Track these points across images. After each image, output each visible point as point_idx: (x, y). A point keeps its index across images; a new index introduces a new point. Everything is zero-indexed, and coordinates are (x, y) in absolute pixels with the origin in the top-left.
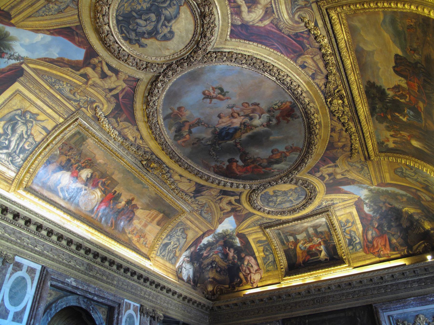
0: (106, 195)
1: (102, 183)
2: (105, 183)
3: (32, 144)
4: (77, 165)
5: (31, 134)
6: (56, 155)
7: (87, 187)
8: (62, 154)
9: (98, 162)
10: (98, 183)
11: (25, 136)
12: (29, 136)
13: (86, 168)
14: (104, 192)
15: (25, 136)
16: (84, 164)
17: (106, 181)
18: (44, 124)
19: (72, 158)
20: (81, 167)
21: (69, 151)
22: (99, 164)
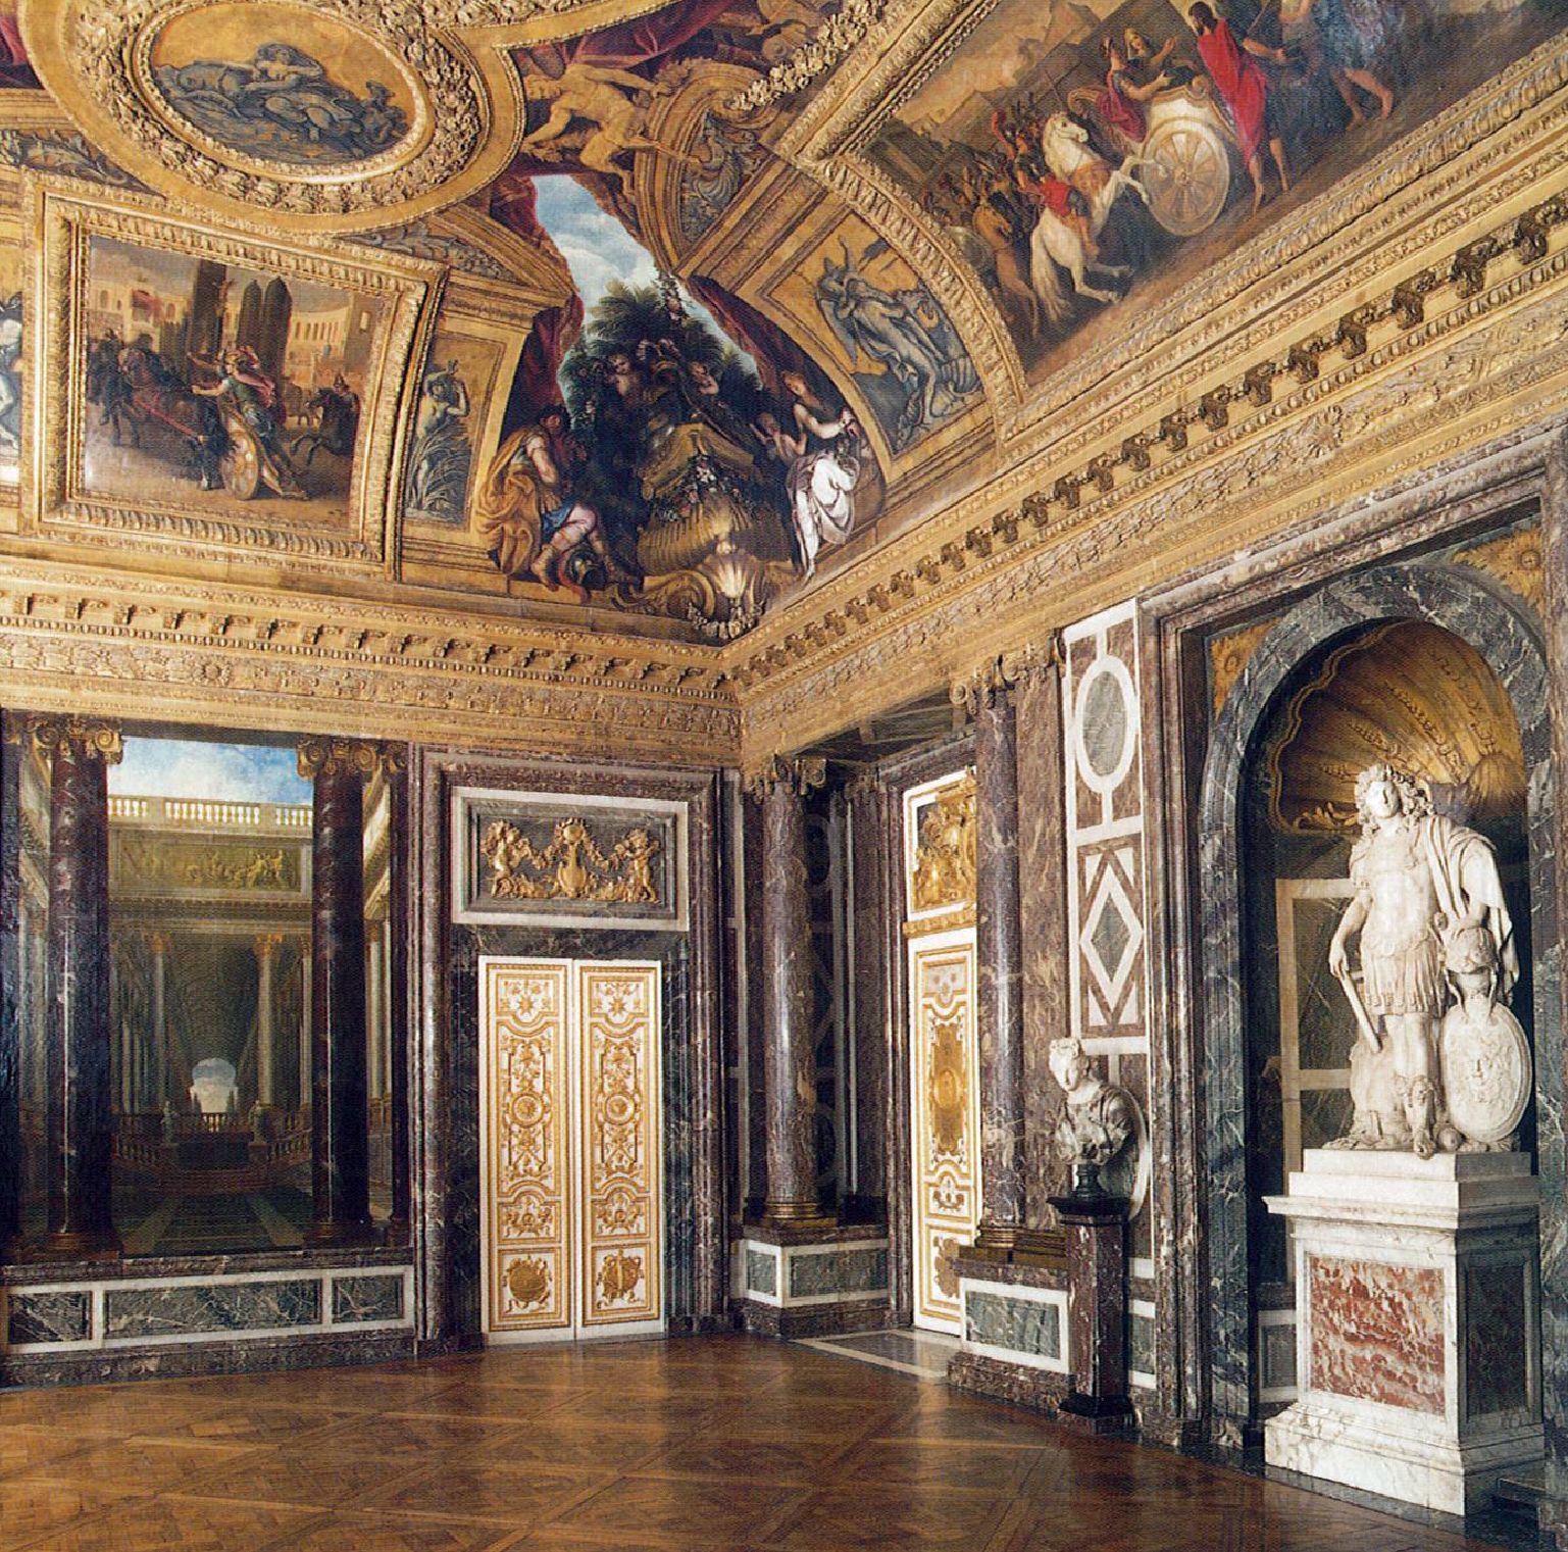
0: (1203, 71)
1: (1134, 81)
2: (1135, 63)
3: (923, 303)
4: (1020, 176)
5: (894, 295)
6: (969, 242)
7: (1129, 161)
8: (967, 219)
9: (1012, 82)
10: (1121, 94)
11: (898, 313)
12: (898, 304)
13: (1039, 140)
14: (1181, 78)
15: (898, 313)
16: (1019, 142)
17: (1122, 55)
18: (857, 254)
19: (988, 186)
20: (1032, 159)
21: (958, 192)
22: (1026, 80)
